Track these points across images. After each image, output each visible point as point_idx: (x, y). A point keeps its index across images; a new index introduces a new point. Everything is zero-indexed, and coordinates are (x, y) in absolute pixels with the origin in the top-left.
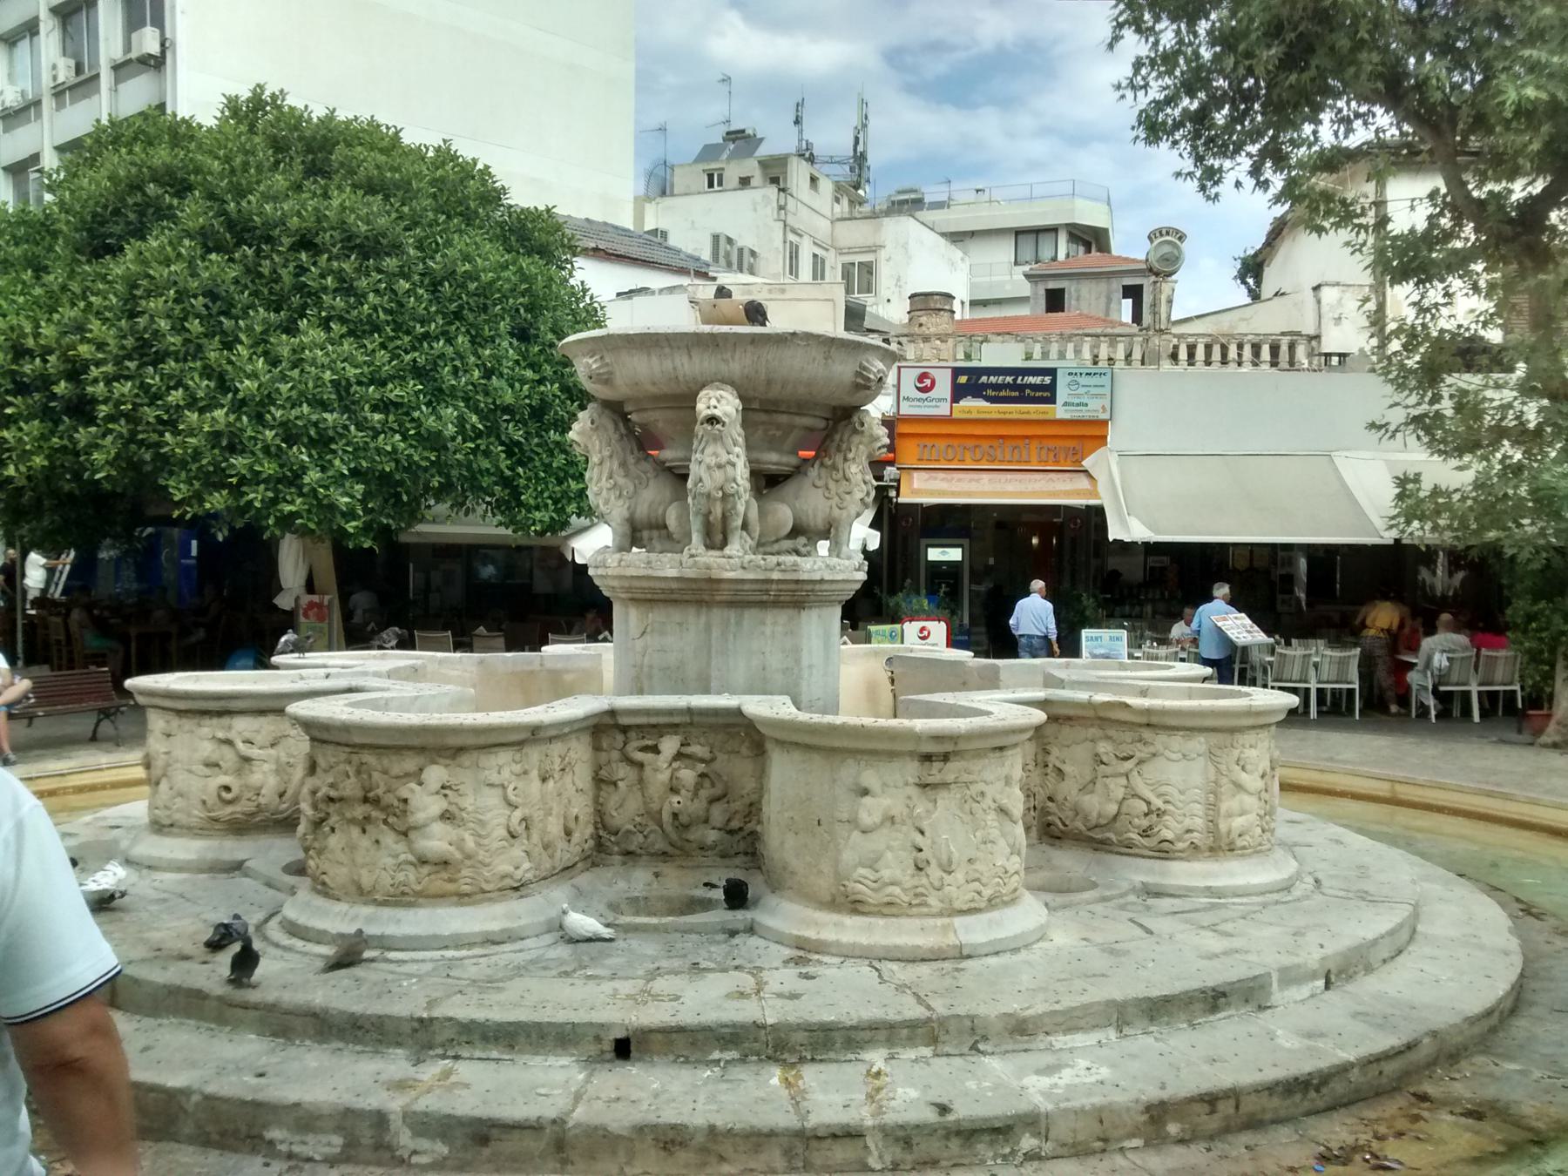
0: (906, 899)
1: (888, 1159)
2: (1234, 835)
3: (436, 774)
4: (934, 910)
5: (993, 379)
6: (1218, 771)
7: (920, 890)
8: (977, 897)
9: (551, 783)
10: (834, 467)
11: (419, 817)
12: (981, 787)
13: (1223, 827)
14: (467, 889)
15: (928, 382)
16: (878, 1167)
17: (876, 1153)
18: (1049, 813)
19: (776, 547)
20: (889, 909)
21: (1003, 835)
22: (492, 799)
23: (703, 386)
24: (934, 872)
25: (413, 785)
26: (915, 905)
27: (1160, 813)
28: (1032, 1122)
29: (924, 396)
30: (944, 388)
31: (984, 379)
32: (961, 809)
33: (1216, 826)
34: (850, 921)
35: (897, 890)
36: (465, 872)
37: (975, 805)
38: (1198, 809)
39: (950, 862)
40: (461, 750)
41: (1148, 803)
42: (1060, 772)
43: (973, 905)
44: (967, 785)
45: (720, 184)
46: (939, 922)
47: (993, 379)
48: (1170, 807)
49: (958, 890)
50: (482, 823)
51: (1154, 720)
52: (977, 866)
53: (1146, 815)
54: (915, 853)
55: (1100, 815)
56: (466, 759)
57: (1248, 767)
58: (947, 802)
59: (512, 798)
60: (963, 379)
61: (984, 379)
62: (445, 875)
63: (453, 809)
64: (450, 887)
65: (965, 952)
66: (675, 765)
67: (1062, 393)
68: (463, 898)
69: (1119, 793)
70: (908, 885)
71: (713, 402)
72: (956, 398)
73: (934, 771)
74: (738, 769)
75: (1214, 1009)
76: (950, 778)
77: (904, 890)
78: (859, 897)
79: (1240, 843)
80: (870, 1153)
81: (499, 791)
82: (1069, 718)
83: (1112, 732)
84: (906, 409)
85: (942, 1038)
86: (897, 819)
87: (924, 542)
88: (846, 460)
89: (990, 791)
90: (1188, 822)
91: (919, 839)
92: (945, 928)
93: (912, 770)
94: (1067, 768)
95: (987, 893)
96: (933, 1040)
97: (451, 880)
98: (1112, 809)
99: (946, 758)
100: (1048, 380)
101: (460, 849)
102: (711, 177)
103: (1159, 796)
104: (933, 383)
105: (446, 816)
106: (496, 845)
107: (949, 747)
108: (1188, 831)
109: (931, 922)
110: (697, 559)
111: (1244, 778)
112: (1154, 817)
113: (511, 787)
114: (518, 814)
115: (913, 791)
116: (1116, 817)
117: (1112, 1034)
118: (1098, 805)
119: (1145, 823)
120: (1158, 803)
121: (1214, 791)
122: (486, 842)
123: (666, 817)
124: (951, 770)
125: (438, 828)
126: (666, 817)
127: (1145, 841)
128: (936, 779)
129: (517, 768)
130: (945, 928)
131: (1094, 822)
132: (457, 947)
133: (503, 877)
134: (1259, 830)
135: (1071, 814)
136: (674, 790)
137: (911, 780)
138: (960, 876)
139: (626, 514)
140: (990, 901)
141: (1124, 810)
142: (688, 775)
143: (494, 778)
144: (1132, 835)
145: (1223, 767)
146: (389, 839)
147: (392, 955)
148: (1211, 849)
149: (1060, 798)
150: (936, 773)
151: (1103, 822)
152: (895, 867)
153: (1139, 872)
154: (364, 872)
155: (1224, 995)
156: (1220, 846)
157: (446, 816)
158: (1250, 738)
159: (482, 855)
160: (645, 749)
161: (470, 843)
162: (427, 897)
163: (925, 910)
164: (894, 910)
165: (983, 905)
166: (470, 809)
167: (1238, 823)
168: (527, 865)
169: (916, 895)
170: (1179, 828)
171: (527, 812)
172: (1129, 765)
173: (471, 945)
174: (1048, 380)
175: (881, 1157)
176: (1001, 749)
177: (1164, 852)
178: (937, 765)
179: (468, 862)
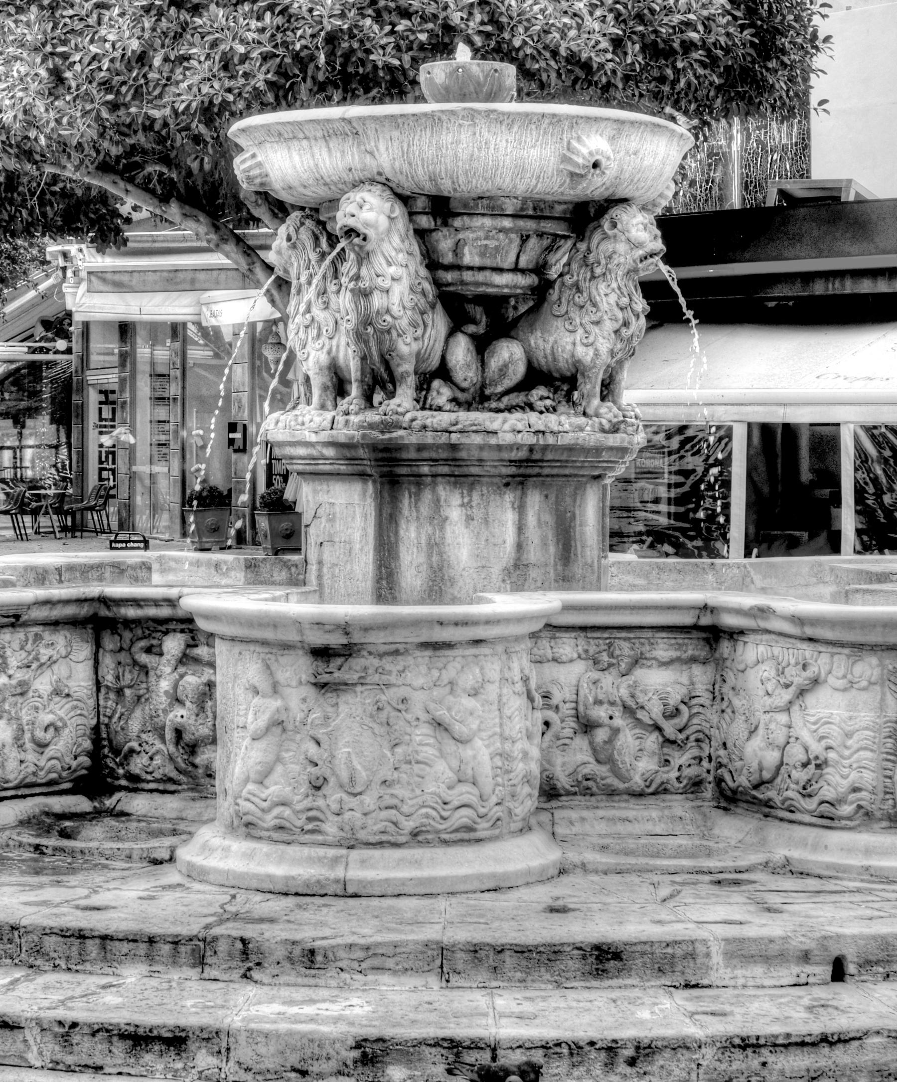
0: (299, 823)
1: (48, 1056)
8: (391, 828)
12: (403, 692)
16: (38, 1064)
17: (35, 1049)
19: (505, 400)
37: (394, 714)
39: (352, 779)
43: (384, 838)
46: (332, 852)
48: (832, 755)
52: (398, 791)
53: (805, 765)
58: (351, 708)
65: (351, 890)
66: (181, 670)
70: (299, 807)
75: (599, 973)
76: (354, 677)
80: (28, 1047)
85: (208, 960)
88: (593, 277)
89: (418, 699)
92: (335, 860)
95: (409, 825)
96: (200, 961)
108: (856, 790)
109: (321, 851)
117: (434, 981)
118: (756, 753)
119: (801, 775)
120: (816, 748)
124: (350, 671)
130: (335, 860)
138: (369, 800)
139: (324, 358)
140: (415, 834)
151: (767, 775)
153: (787, 843)
155: (617, 956)
160: (148, 650)
163: (320, 838)
165: (402, 839)
169: (310, 819)
170: (845, 784)
175: (41, 1054)
177: (828, 820)
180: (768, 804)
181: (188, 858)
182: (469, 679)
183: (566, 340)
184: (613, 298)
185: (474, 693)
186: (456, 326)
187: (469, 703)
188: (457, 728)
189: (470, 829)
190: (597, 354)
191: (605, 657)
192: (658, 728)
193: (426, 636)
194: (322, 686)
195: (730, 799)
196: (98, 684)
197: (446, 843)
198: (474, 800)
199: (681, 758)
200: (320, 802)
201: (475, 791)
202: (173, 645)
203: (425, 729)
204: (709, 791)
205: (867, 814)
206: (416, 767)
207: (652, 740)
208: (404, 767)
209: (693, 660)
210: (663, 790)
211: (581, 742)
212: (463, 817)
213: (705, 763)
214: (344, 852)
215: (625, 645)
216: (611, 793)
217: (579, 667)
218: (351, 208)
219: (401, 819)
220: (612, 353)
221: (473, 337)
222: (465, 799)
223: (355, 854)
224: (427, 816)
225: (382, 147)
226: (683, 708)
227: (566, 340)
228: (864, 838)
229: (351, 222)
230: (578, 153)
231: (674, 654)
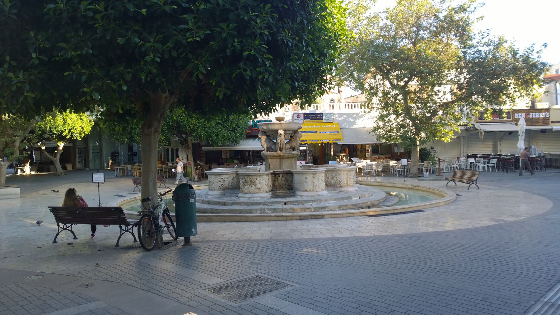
3: (258, 178)
20: (310, 191)
22: (264, 181)
26: (313, 191)
28: (327, 207)
30: (302, 117)
58: (316, 179)
67: (324, 118)
72: (304, 119)
74: (289, 177)
110: (278, 152)
121: (347, 179)
142: (283, 179)
146: (253, 186)
150: (315, 176)
152: (311, 187)
156: (348, 185)
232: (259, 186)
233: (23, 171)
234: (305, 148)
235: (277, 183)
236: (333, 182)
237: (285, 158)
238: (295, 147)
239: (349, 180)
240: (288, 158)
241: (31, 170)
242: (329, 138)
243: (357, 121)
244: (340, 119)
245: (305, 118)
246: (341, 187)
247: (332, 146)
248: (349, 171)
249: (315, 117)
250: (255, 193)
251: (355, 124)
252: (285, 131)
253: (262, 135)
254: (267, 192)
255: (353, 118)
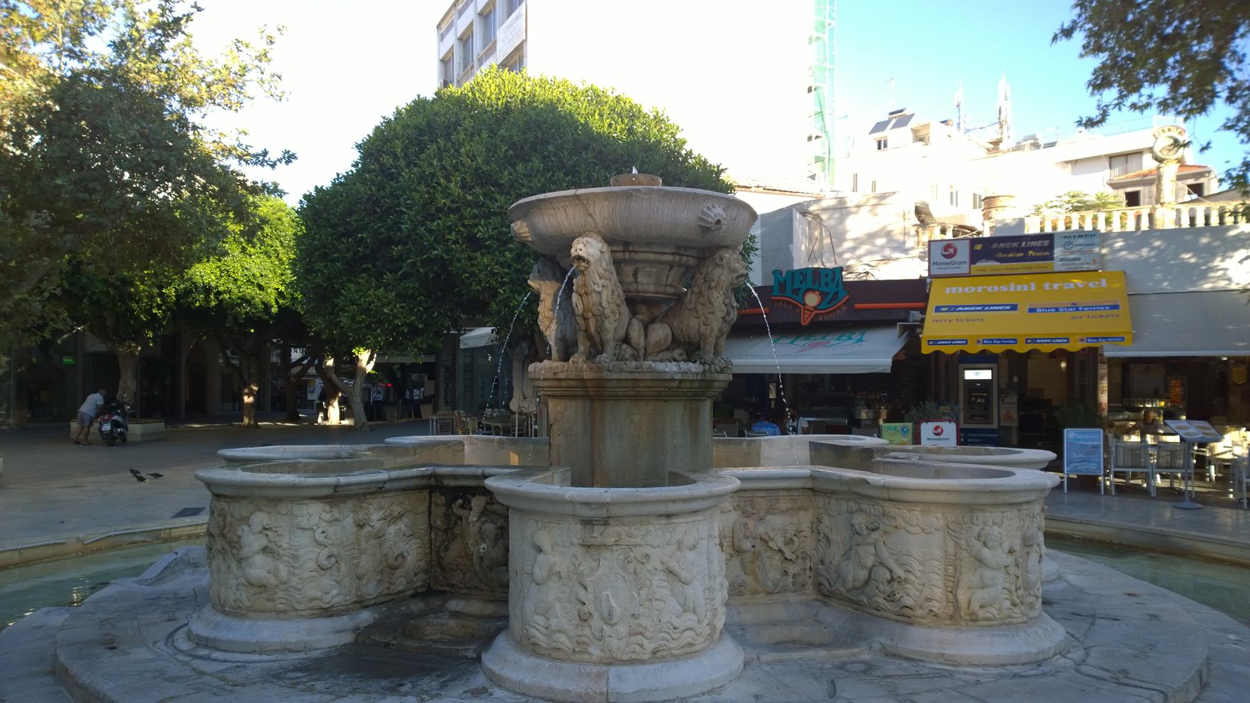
0: (571, 646)
2: (975, 606)
4: (595, 658)
5: (1002, 245)
6: (957, 545)
7: (583, 639)
8: (638, 649)
9: (367, 529)
10: (700, 293)
11: (245, 551)
13: (962, 596)
14: (281, 607)
15: (951, 251)
18: (820, 575)
20: (553, 654)
21: (673, 594)
23: (580, 235)
24: (596, 622)
25: (245, 527)
27: (901, 581)
29: (949, 260)
30: (964, 254)
31: (995, 245)
32: (624, 569)
33: (955, 597)
34: (527, 661)
35: (563, 638)
36: (280, 594)
37: (639, 565)
38: (938, 580)
39: (610, 614)
40: (280, 500)
41: (891, 571)
42: (828, 541)
43: (634, 656)
44: (631, 547)
45: (885, 146)
46: (595, 670)
47: (1002, 245)
49: (617, 640)
50: (295, 557)
51: (893, 495)
52: (642, 621)
53: (889, 582)
54: (579, 606)
55: (855, 580)
56: (283, 508)
57: (990, 543)
58: (610, 560)
59: (320, 538)
60: (979, 247)
61: (995, 245)
62: (265, 596)
63: (272, 546)
64: (270, 605)
67: (1058, 252)
68: (280, 614)
69: (870, 561)
71: (581, 246)
73: (595, 534)
77: (569, 638)
78: (535, 640)
79: (981, 614)
81: (310, 533)
82: (834, 492)
83: (865, 506)
84: (935, 271)
86: (563, 575)
87: (961, 366)
88: (710, 288)
89: (656, 554)
90: (927, 592)
91: (582, 594)
92: (600, 675)
93: (576, 531)
94: (833, 537)
95: (650, 646)
97: (270, 600)
98: (863, 574)
99: (606, 522)
100: (1046, 243)
101: (276, 576)
102: (879, 143)
103: (902, 565)
104: (955, 251)
105: (265, 550)
106: (306, 574)
107: (603, 513)
108: (928, 600)
111: (986, 553)
112: (895, 584)
113: (320, 530)
114: (326, 552)
115: (579, 551)
116: (867, 582)
119: (888, 589)
120: (900, 572)
121: (953, 565)
122: (298, 571)
123: (476, 560)
124: (611, 534)
125: (259, 559)
126: (476, 560)
127: (889, 605)
128: (599, 540)
129: (327, 516)
130: (600, 675)
131: (850, 585)
132: (261, 653)
133: (312, 600)
134: (1008, 604)
135: (834, 576)
136: (483, 539)
137: (575, 541)
138: (622, 629)
140: (654, 653)
141: (873, 576)
142: (490, 528)
143: (305, 523)
144: (880, 600)
145: (963, 542)
146: (234, 566)
147: (216, 655)
148: (951, 617)
149: (827, 561)
152: (563, 618)
154: (223, 589)
156: (957, 617)
157: (265, 550)
158: (996, 515)
159: (294, 581)
160: (462, 507)
161: (284, 573)
162: (255, 611)
163: (587, 657)
164: (555, 654)
165: (646, 657)
166: (285, 546)
167: (980, 596)
168: (335, 592)
171: (335, 551)
172: (875, 535)
173: (271, 652)
174: (1046, 243)
176: (669, 516)
178: (598, 529)
179: (282, 587)
180: (859, 603)
181: (490, 665)
182: (689, 540)
183: (694, 322)
184: (721, 299)
185: (694, 547)
186: (634, 313)
187: (690, 555)
188: (684, 575)
189: (692, 645)
190: (712, 330)
191: (749, 508)
192: (780, 551)
193: (662, 509)
194: (588, 547)
195: (825, 594)
196: (431, 527)
197: (678, 657)
198: (694, 624)
199: (792, 569)
200: (587, 631)
201: (694, 617)
202: (477, 503)
203: (662, 576)
204: (810, 588)
205: (936, 615)
206: (655, 603)
207: (777, 558)
208: (647, 604)
209: (801, 508)
210: (784, 590)
211: (736, 562)
212: (688, 637)
213: (808, 573)
214: (605, 668)
215: (761, 501)
216: (755, 592)
217: (734, 516)
218: (581, 246)
219: (645, 642)
220: (720, 330)
221: (642, 321)
222: (689, 624)
223: (613, 671)
224: (663, 639)
225: (597, 211)
226: (795, 539)
227: (694, 322)
228: (936, 634)
229: (581, 253)
230: (708, 216)
231: (789, 505)
232: (259, 568)
233: (326, 418)
234: (986, 375)
235: (456, 548)
236: (854, 573)
237: (616, 398)
238: (702, 337)
239: (968, 577)
240: (636, 397)
241: (342, 417)
242: (1072, 331)
243: (1217, 262)
244: (1132, 257)
245: (975, 257)
246: (905, 617)
247: (1103, 370)
248: (972, 508)
249: (1019, 250)
250: (238, 612)
251: (1204, 276)
252: (609, 240)
253: (542, 276)
254: (327, 612)
255: (1197, 251)
